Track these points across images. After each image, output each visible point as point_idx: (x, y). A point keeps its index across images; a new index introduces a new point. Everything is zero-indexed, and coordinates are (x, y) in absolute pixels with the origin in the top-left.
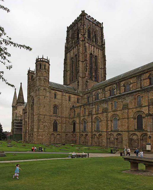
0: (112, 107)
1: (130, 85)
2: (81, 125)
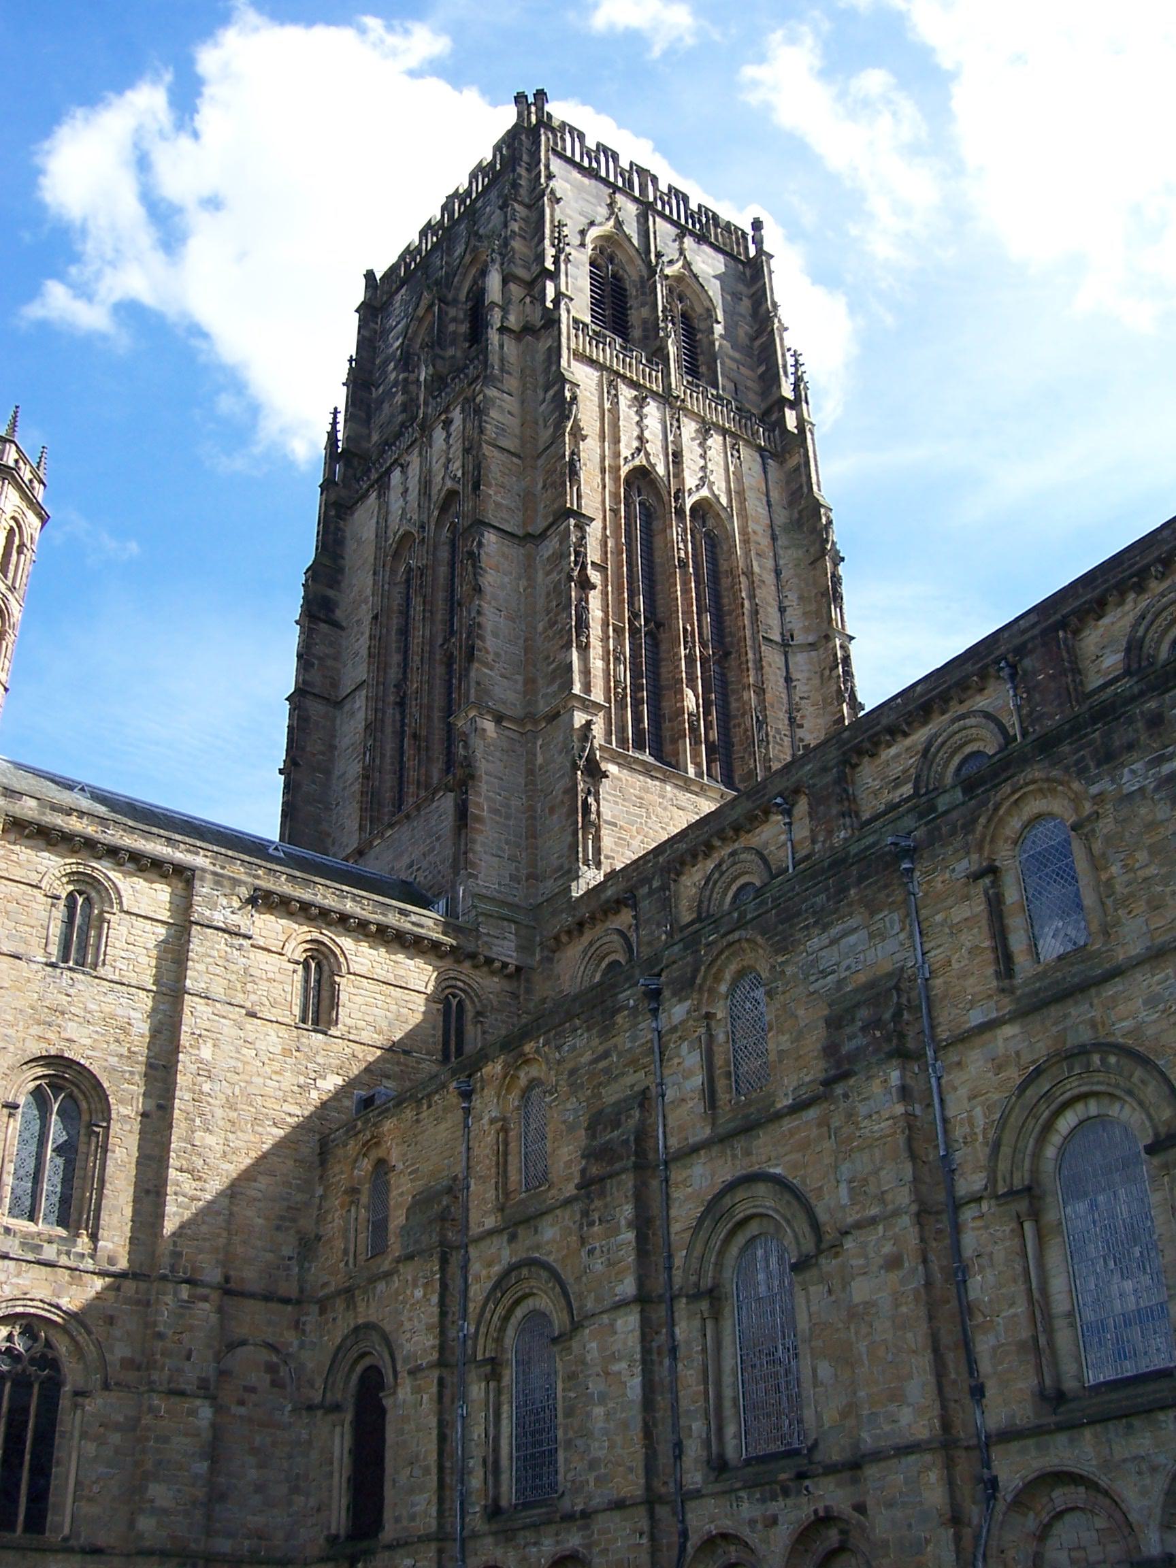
0: (1000, 933)
2: (477, 1391)
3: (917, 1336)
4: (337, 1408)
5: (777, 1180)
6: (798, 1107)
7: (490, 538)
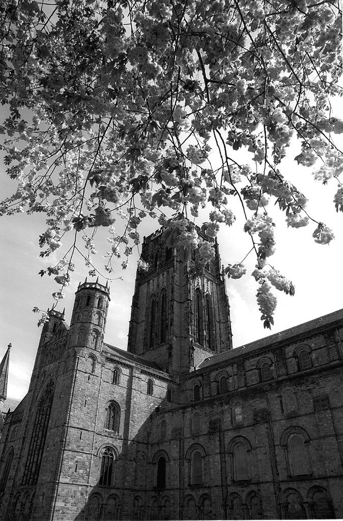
0: (282, 406)
1: (310, 353)
2: (186, 464)
3: (269, 465)
4: (155, 464)
5: (244, 437)
7: (175, 302)
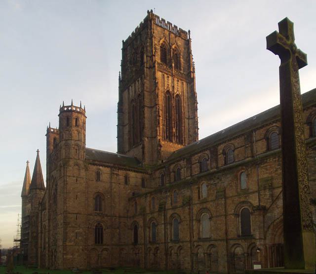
6: (180, 207)
